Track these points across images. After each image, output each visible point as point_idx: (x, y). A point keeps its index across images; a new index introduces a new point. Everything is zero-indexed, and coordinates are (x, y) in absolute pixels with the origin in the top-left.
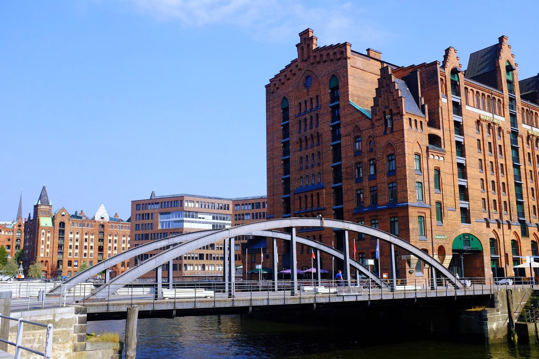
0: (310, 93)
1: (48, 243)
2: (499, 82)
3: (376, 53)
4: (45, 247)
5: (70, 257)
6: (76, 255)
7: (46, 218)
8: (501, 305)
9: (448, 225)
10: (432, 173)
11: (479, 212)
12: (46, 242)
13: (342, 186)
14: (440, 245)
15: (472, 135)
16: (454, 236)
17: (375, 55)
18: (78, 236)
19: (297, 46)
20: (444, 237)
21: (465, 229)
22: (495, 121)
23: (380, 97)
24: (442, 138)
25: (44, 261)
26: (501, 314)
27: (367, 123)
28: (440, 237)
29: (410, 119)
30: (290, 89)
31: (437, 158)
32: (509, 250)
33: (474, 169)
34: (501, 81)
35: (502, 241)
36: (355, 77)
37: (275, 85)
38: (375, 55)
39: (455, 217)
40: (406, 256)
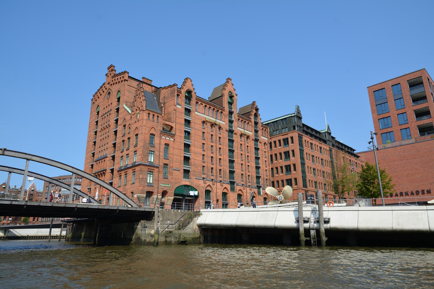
0: (109, 102)
2: (223, 103)
3: (148, 80)
8: (161, 219)
9: (172, 179)
10: (163, 146)
11: (198, 173)
13: (115, 155)
14: (164, 190)
15: (199, 129)
16: (177, 186)
17: (148, 81)
19: (106, 75)
20: (168, 186)
21: (186, 182)
22: (217, 123)
23: (136, 101)
24: (174, 127)
26: (160, 224)
27: (129, 116)
28: (165, 185)
29: (149, 114)
30: (101, 101)
32: (220, 197)
33: (198, 148)
34: (224, 102)
35: (215, 192)
36: (129, 91)
37: (95, 98)
38: (148, 81)
39: (179, 174)
40: (137, 195)
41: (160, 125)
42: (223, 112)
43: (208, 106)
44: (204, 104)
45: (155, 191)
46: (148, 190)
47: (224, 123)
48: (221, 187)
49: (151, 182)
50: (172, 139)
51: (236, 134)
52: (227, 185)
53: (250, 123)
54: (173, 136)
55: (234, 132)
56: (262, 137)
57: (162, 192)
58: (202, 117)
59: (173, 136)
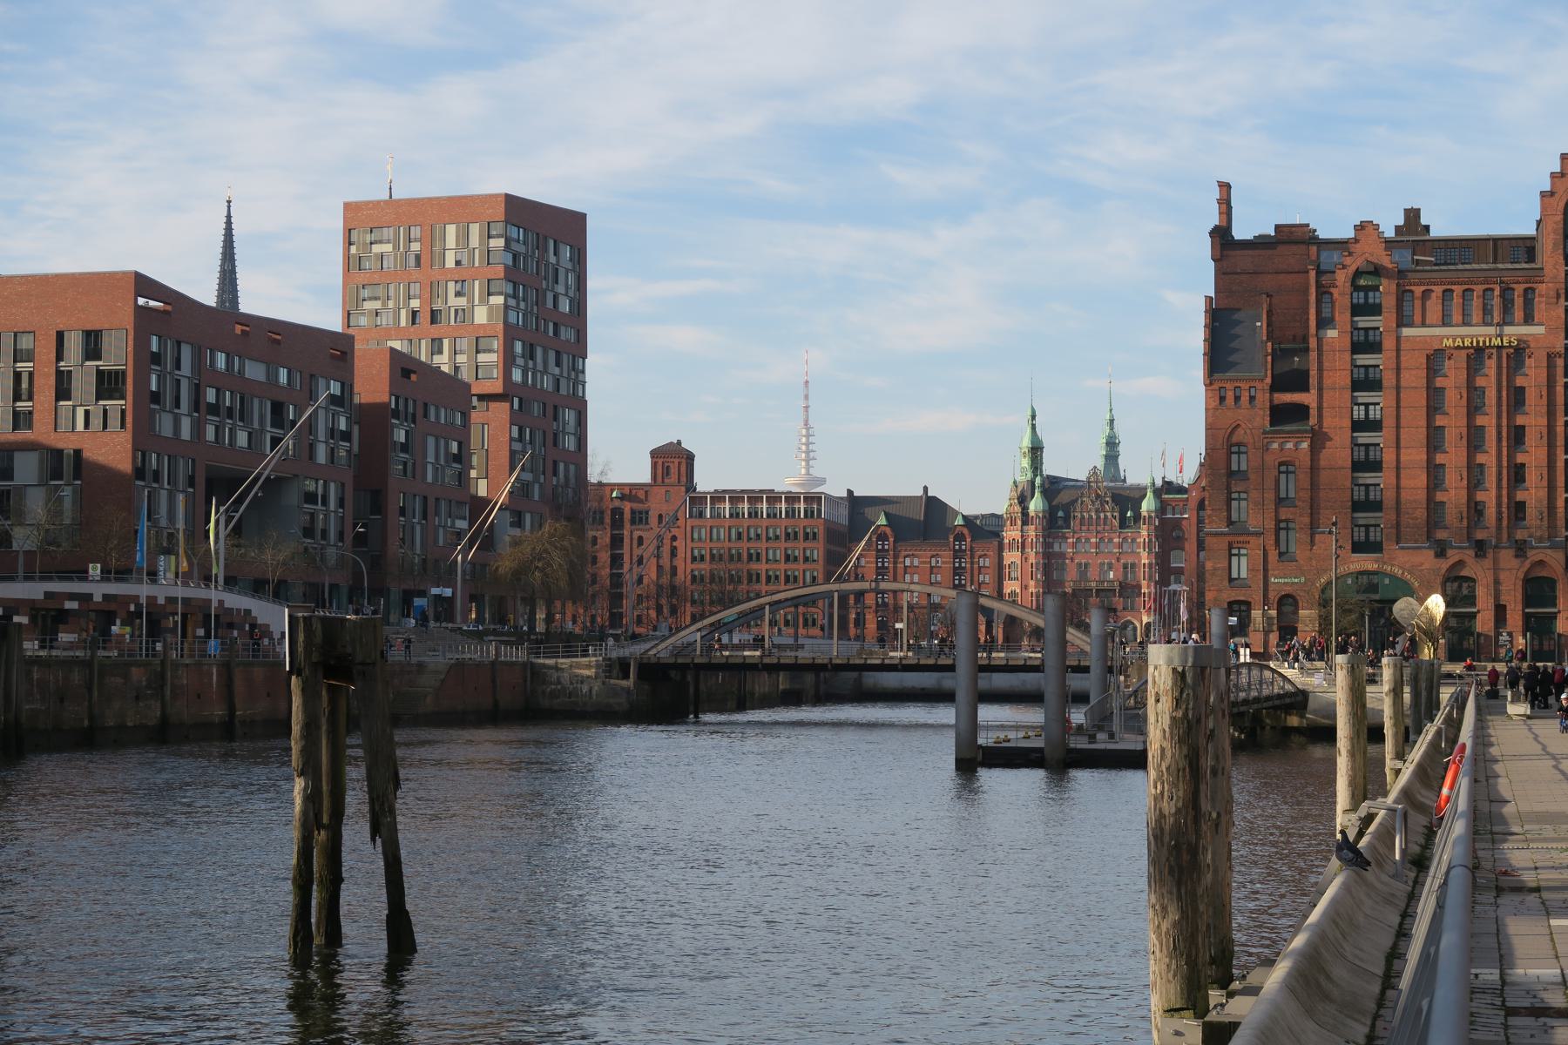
15: (1413, 385)
24: (1313, 405)
33: (1409, 451)
41: (1261, 413)
43: (1458, 289)
45: (1256, 596)
46: (1232, 599)
47: (1540, 330)
48: (1515, 563)
52: (1549, 551)
57: (1276, 600)
58: (1428, 339)
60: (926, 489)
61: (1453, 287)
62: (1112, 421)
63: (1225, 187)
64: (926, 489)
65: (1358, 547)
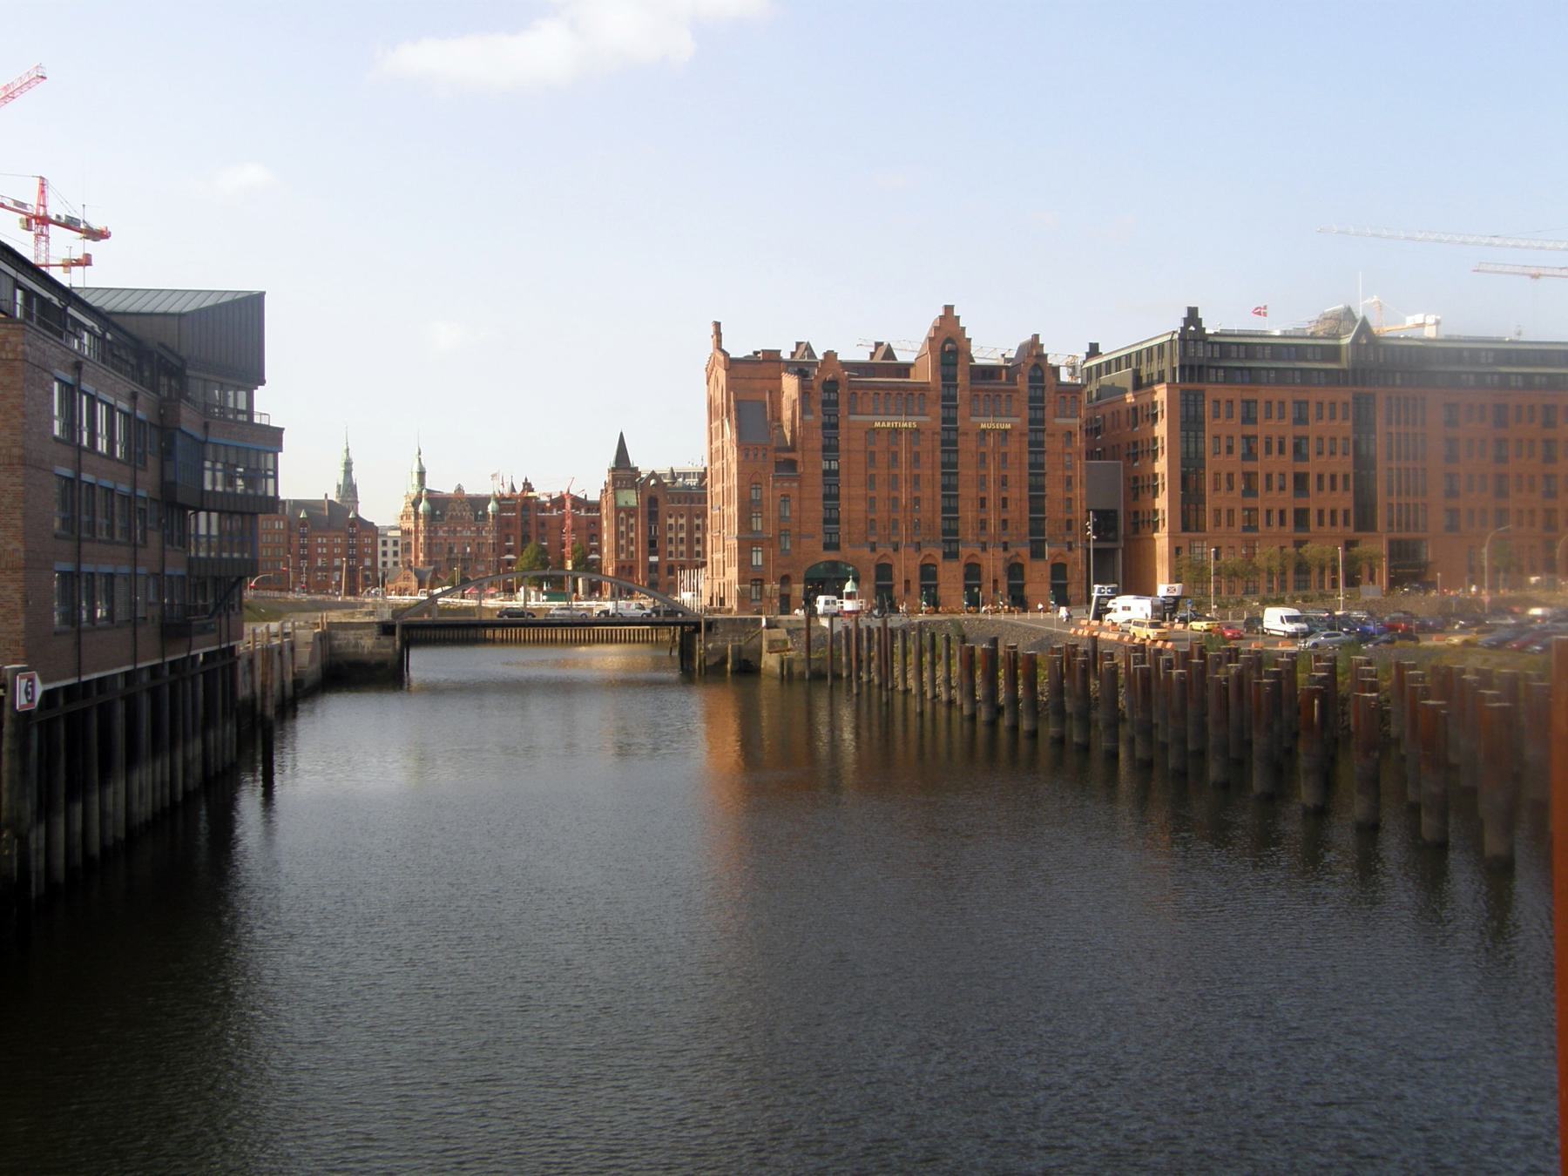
1: (632, 535)
4: (627, 542)
5: (671, 559)
6: (682, 555)
7: (625, 491)
12: (628, 534)
16: (809, 564)
18: (682, 521)
21: (832, 556)
25: (627, 566)
31: (786, 485)
42: (927, 393)
44: (871, 393)
48: (916, 555)
49: (760, 563)
50: (795, 485)
51: (966, 434)
53: (1015, 396)
54: (799, 479)
55: (960, 431)
56: (1058, 421)
59: (799, 479)
60: (326, 495)
61: (880, 392)
62: (348, 450)
63: (717, 325)
64: (326, 495)
65: (827, 547)
